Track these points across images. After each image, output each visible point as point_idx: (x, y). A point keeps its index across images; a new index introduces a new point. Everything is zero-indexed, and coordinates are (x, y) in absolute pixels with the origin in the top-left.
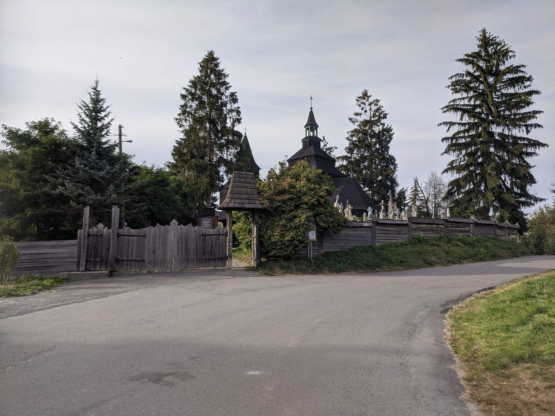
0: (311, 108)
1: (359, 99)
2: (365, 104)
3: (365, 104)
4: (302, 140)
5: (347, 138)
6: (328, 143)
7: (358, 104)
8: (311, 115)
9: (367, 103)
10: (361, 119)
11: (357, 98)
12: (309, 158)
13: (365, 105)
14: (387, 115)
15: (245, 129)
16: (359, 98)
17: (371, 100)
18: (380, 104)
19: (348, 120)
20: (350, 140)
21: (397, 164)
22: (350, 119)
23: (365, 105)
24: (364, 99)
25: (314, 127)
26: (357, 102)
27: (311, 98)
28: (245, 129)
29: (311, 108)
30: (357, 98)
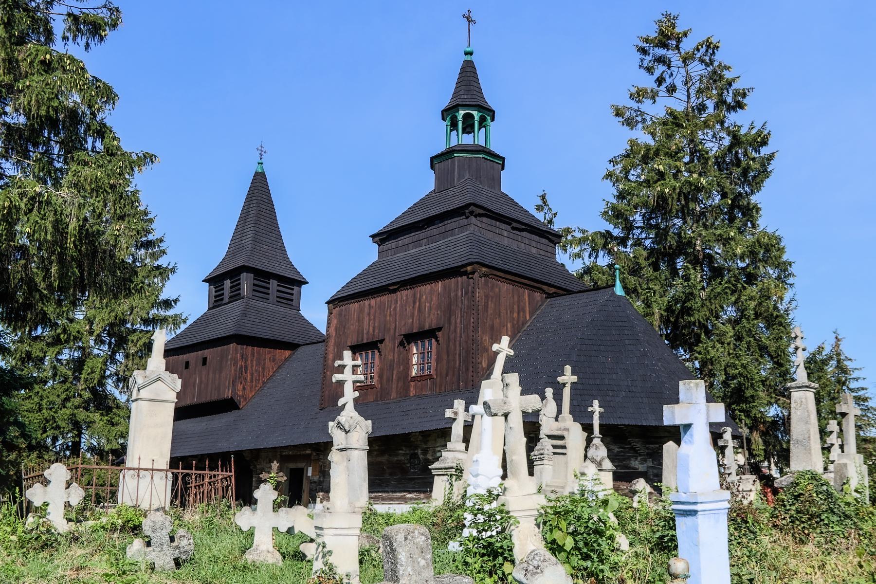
1: (645, 45)
2: (667, 63)
3: (667, 63)
6: (555, 214)
7: (645, 64)
9: (676, 59)
10: (656, 110)
13: (669, 67)
15: (262, 150)
17: (687, 46)
18: (719, 57)
21: (790, 264)
23: (669, 67)
24: (665, 46)
26: (639, 56)
27: (469, 19)
28: (262, 150)
30: (641, 44)
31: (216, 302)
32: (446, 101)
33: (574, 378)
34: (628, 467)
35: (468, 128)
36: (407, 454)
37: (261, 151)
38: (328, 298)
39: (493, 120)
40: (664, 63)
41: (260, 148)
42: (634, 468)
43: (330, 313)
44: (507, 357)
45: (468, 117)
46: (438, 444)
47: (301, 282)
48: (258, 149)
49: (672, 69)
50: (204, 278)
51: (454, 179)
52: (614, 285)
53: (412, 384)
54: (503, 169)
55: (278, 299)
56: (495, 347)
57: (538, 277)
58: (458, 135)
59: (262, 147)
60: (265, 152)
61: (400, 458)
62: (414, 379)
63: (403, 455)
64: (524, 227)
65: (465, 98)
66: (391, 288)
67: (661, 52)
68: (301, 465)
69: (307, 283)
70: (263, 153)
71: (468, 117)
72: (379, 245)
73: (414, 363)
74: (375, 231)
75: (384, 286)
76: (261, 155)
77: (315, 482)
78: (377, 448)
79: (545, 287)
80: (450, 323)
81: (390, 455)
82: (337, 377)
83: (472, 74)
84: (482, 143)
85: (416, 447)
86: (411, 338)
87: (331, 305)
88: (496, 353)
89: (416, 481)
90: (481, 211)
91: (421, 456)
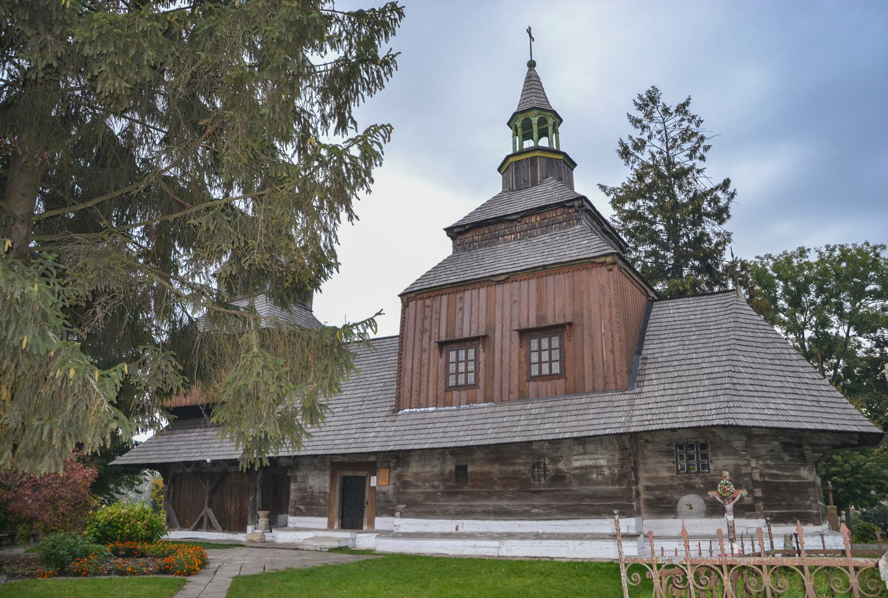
0: (532, 64)
8: (533, 83)
25: (551, 121)
29: (532, 64)
34: (798, 477)
36: (528, 463)
38: (401, 291)
42: (804, 479)
43: (405, 306)
45: (542, 121)
46: (575, 452)
51: (537, 177)
61: (517, 468)
62: (534, 379)
63: (523, 464)
64: (609, 230)
66: (496, 279)
68: (360, 474)
74: (449, 224)
77: (384, 493)
78: (482, 456)
81: (503, 464)
85: (542, 456)
87: (405, 298)
89: (544, 494)
90: (589, 207)
91: (549, 467)
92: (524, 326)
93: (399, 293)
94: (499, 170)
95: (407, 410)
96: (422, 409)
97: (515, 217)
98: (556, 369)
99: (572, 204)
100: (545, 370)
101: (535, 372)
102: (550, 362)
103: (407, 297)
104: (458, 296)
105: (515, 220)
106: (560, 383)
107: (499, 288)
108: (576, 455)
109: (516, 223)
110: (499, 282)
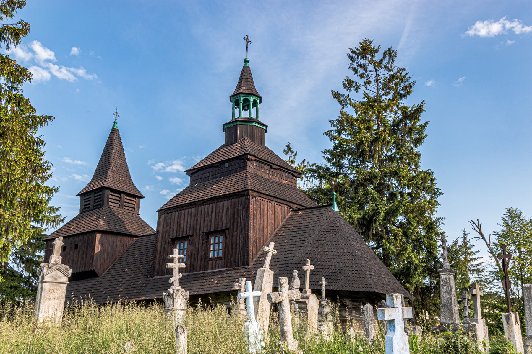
4: (224, 125)
5: (328, 133)
10: (358, 97)
11: (351, 53)
12: (233, 163)
13: (366, 71)
14: (411, 87)
15: (116, 115)
16: (353, 52)
17: (378, 57)
19: (332, 96)
20: (333, 138)
22: (336, 95)
23: (366, 71)
24: (364, 57)
25: (252, 99)
27: (247, 40)
28: (116, 115)
29: (246, 61)
31: (85, 209)
32: (233, 90)
33: (312, 267)
35: (246, 106)
37: (116, 115)
38: (158, 209)
39: (260, 102)
40: (364, 69)
41: (115, 113)
43: (159, 218)
44: (273, 255)
46: (225, 300)
47: (141, 197)
48: (114, 114)
49: (368, 72)
50: (77, 193)
52: (332, 205)
53: (210, 262)
54: (266, 132)
55: (125, 207)
56: (266, 248)
57: (287, 199)
58: (240, 111)
59: (116, 113)
60: (119, 116)
62: (211, 259)
65: (243, 89)
67: (362, 61)
69: (143, 197)
70: (117, 117)
71: (246, 101)
72: (191, 177)
73: (211, 250)
75: (193, 202)
76: (116, 117)
79: (291, 204)
80: (233, 226)
82: (170, 265)
83: (249, 75)
84: (253, 116)
86: (209, 234)
88: (267, 252)
92: (209, 230)
93: (157, 210)
94: (223, 130)
95: (157, 277)
96: (163, 276)
97: (217, 165)
98: (220, 255)
99: (243, 157)
100: (216, 256)
101: (211, 256)
102: (218, 250)
103: (161, 212)
104: (183, 212)
105: (218, 166)
106: (221, 262)
107: (200, 208)
108: (226, 302)
109: (217, 168)
110: (200, 205)
